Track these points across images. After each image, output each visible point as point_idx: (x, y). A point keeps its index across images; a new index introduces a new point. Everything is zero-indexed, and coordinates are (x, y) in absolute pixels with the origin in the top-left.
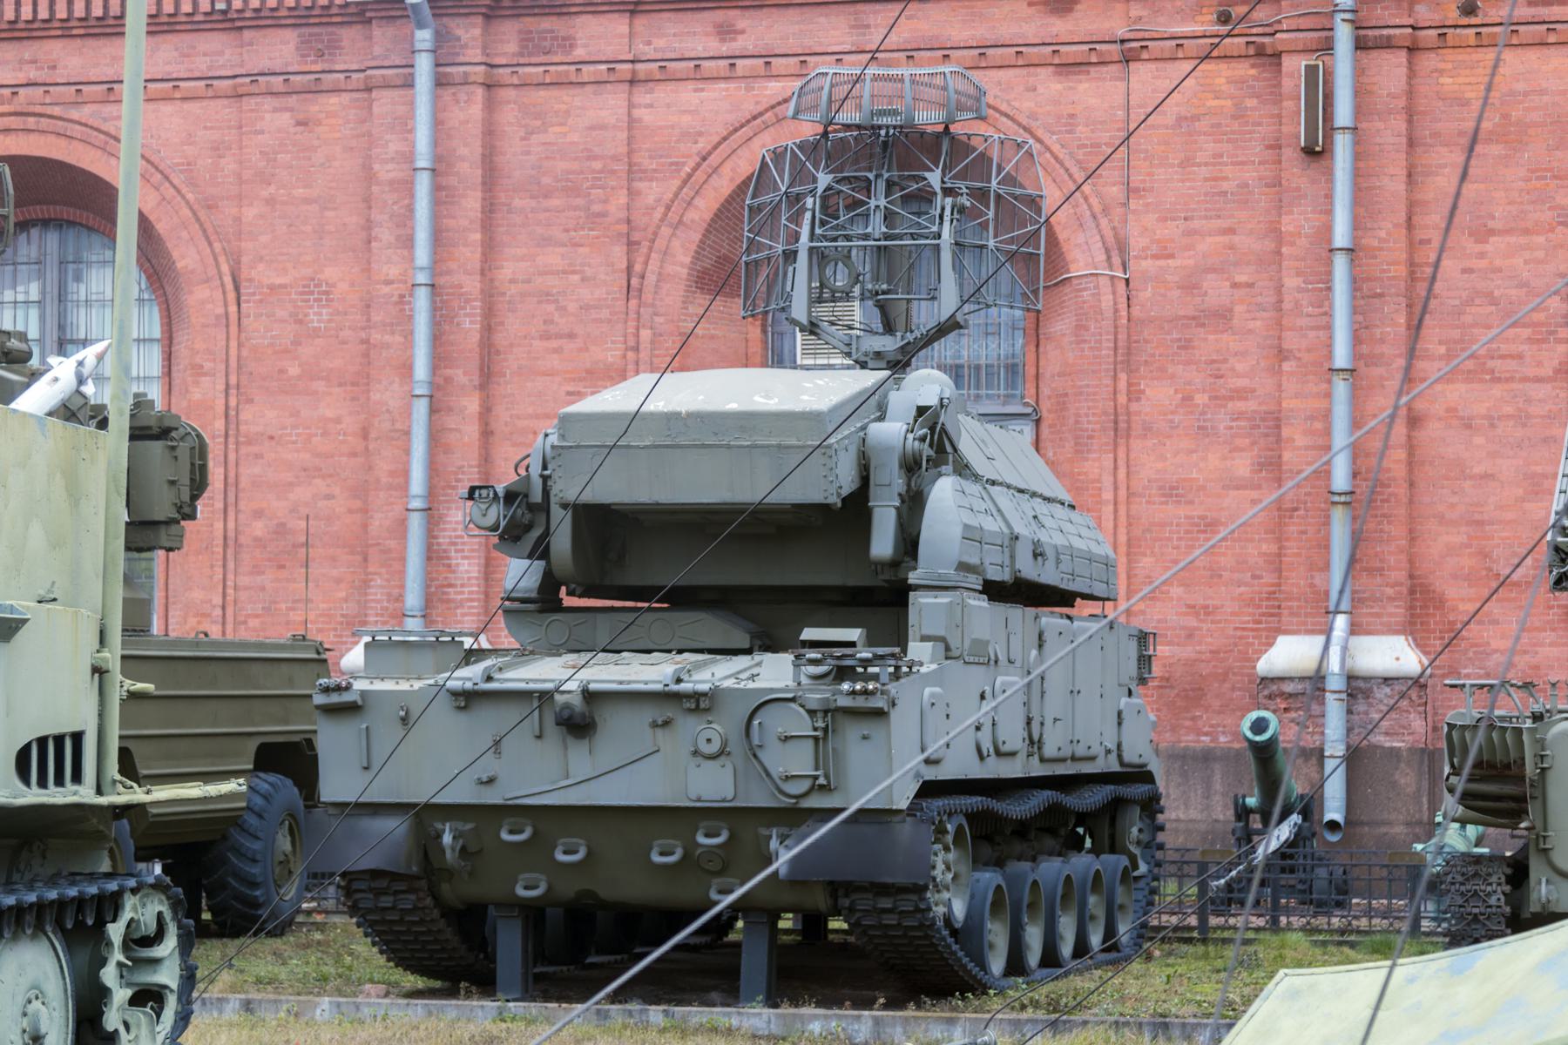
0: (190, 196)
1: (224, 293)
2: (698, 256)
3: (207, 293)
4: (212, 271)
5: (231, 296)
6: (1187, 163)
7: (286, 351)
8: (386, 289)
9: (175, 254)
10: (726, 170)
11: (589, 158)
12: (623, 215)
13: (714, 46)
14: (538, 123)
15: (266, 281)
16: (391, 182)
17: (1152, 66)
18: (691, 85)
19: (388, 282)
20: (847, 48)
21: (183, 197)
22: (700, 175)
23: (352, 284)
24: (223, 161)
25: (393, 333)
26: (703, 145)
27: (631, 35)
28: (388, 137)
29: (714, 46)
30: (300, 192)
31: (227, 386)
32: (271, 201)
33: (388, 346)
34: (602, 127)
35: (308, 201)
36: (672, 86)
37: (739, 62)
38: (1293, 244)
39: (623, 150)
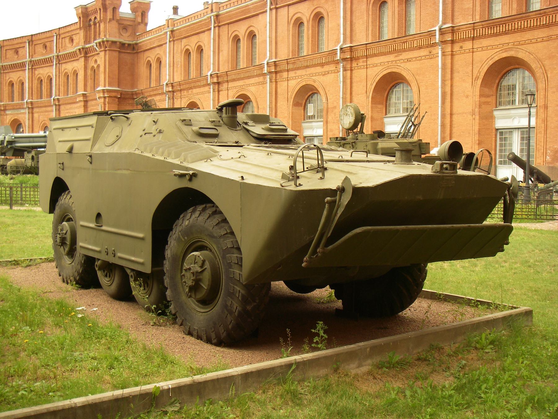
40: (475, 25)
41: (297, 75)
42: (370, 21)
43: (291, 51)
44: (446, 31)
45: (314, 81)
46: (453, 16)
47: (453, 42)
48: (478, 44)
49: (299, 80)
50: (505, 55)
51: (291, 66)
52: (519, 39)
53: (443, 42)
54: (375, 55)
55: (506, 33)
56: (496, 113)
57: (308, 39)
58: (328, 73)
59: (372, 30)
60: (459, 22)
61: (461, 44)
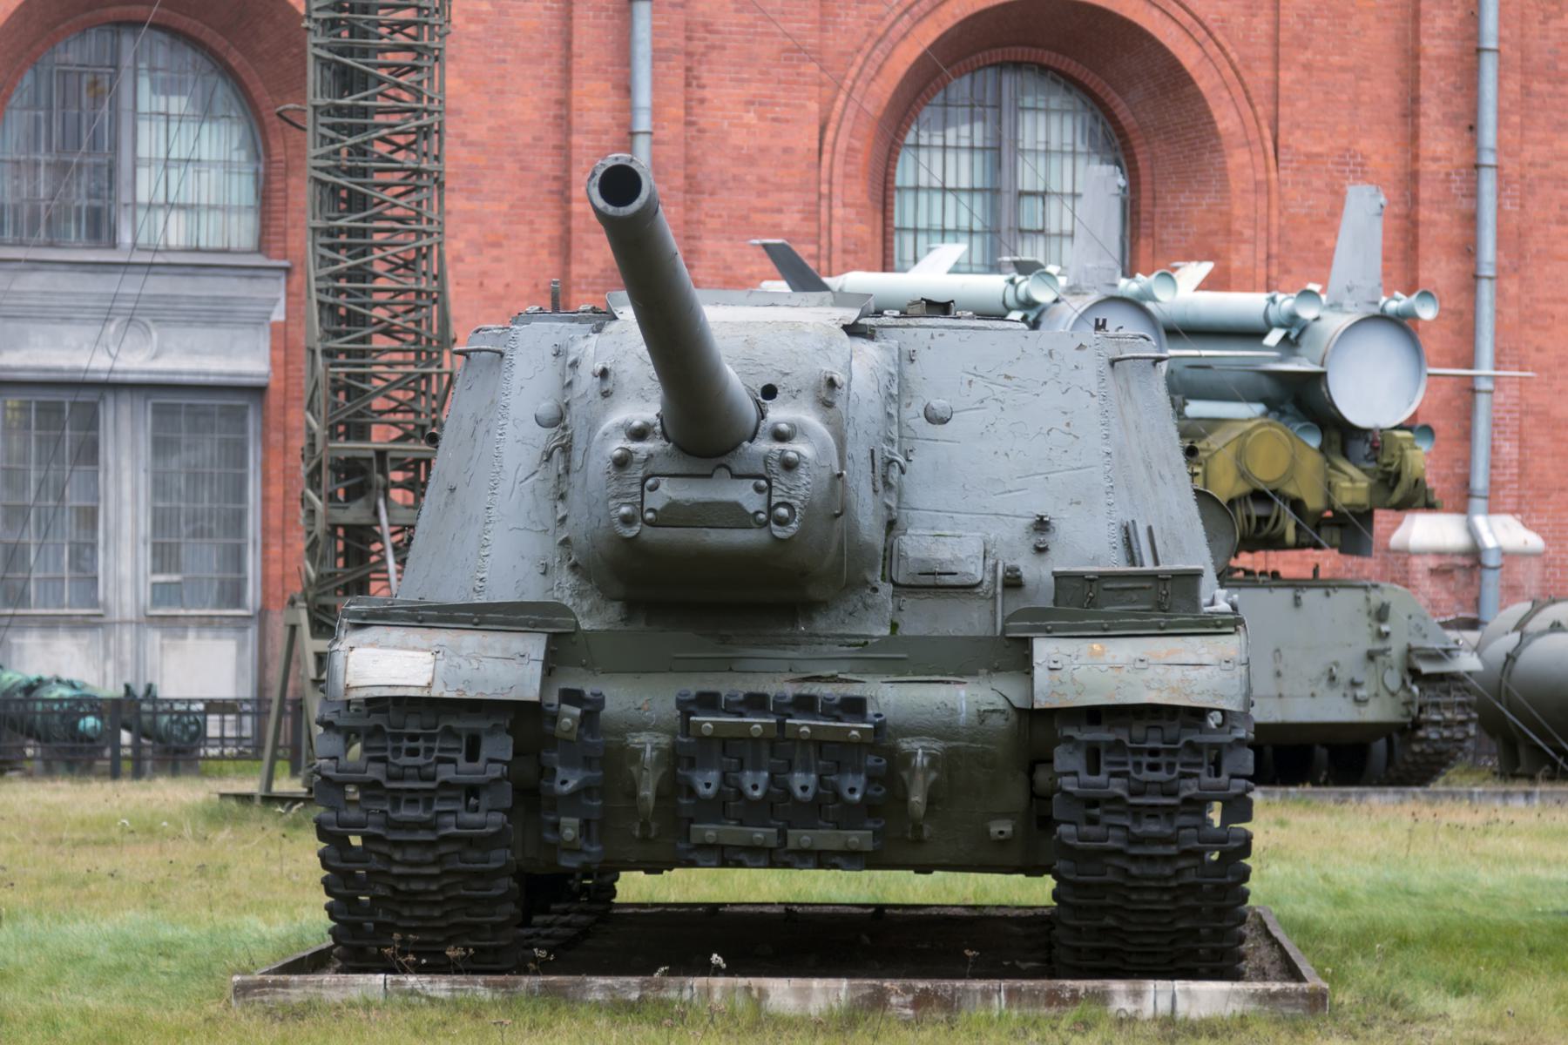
0: (1234, 56)
1: (1266, 157)
3: (1247, 157)
4: (1253, 135)
5: (1272, 162)
7: (1323, 222)
8: (1433, 167)
9: (1216, 115)
14: (1555, 8)
15: (1303, 149)
16: (1438, 58)
19: (1436, 159)
21: (1227, 56)
23: (1386, 158)
24: (1255, 20)
25: (1439, 211)
28: (1436, 12)
30: (1336, 59)
31: (1269, 257)
32: (1307, 67)
33: (1433, 224)
35: (1343, 69)
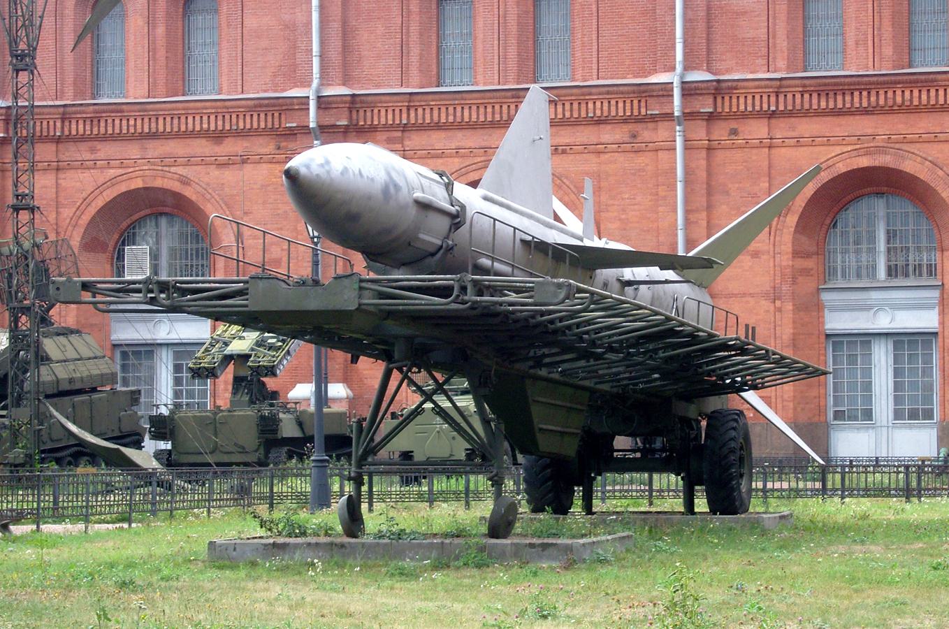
2: (83, 238)
6: (264, 203)
10: (93, 204)
11: (42, 199)
12: (55, 221)
13: (87, 156)
17: (252, 165)
18: (79, 171)
20: (139, 157)
22: (83, 206)
26: (84, 195)
27: (57, 151)
29: (87, 156)
34: (46, 187)
36: (72, 171)
37: (98, 162)
38: (302, 234)
39: (55, 196)
40: (784, 82)
41: (101, 155)
42: (414, 28)
43: (70, 79)
44: (696, 89)
45: (185, 181)
46: (709, 51)
47: (711, 117)
48: (782, 129)
49: (112, 172)
50: (864, 162)
51: (77, 128)
52: (902, 128)
53: (689, 116)
54: (438, 127)
55: (865, 112)
56: (825, 296)
57: (152, 50)
58: (244, 162)
59: (421, 56)
60: (728, 71)
61: (733, 125)
